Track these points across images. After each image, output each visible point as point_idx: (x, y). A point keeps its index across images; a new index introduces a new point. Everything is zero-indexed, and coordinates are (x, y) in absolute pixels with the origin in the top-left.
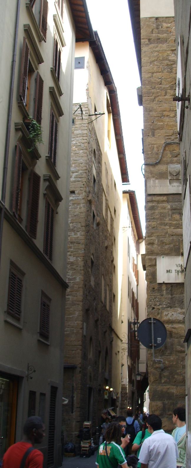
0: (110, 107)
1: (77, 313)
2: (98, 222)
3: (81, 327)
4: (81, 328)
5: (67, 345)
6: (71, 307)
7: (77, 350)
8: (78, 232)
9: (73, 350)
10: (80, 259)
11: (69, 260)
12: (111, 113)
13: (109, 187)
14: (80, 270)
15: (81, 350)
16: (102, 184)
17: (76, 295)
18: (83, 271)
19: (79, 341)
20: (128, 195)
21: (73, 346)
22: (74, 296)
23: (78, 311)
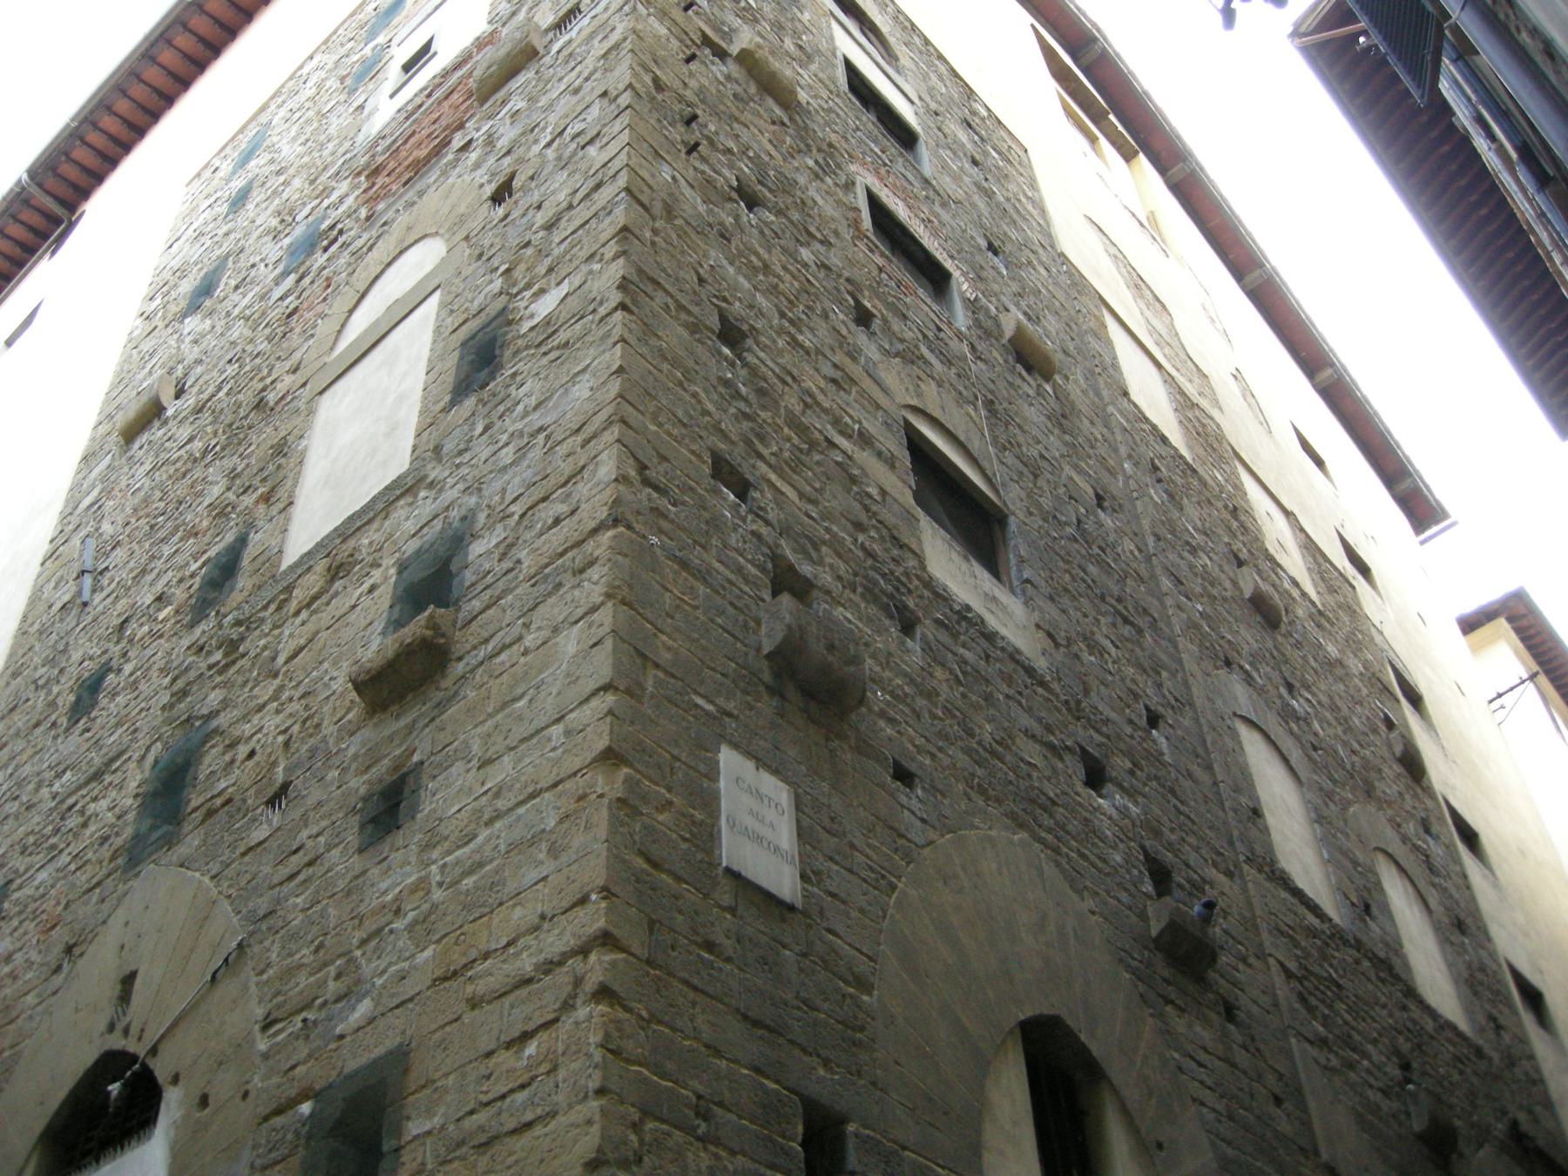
0: (1112, 117)
1: (570, 643)
2: (1009, 331)
3: (602, 744)
4: (610, 757)
5: (474, 1003)
6: (526, 626)
7: (568, 1006)
8: (591, 142)
9: (526, 1036)
10: (597, 267)
11: (526, 326)
12: (1136, 153)
13: (1205, 376)
14: (601, 320)
15: (604, 993)
16: (1062, 255)
17: (562, 508)
18: (619, 315)
19: (583, 901)
20: (1502, 623)
21: (529, 981)
22: (550, 521)
23: (576, 622)
